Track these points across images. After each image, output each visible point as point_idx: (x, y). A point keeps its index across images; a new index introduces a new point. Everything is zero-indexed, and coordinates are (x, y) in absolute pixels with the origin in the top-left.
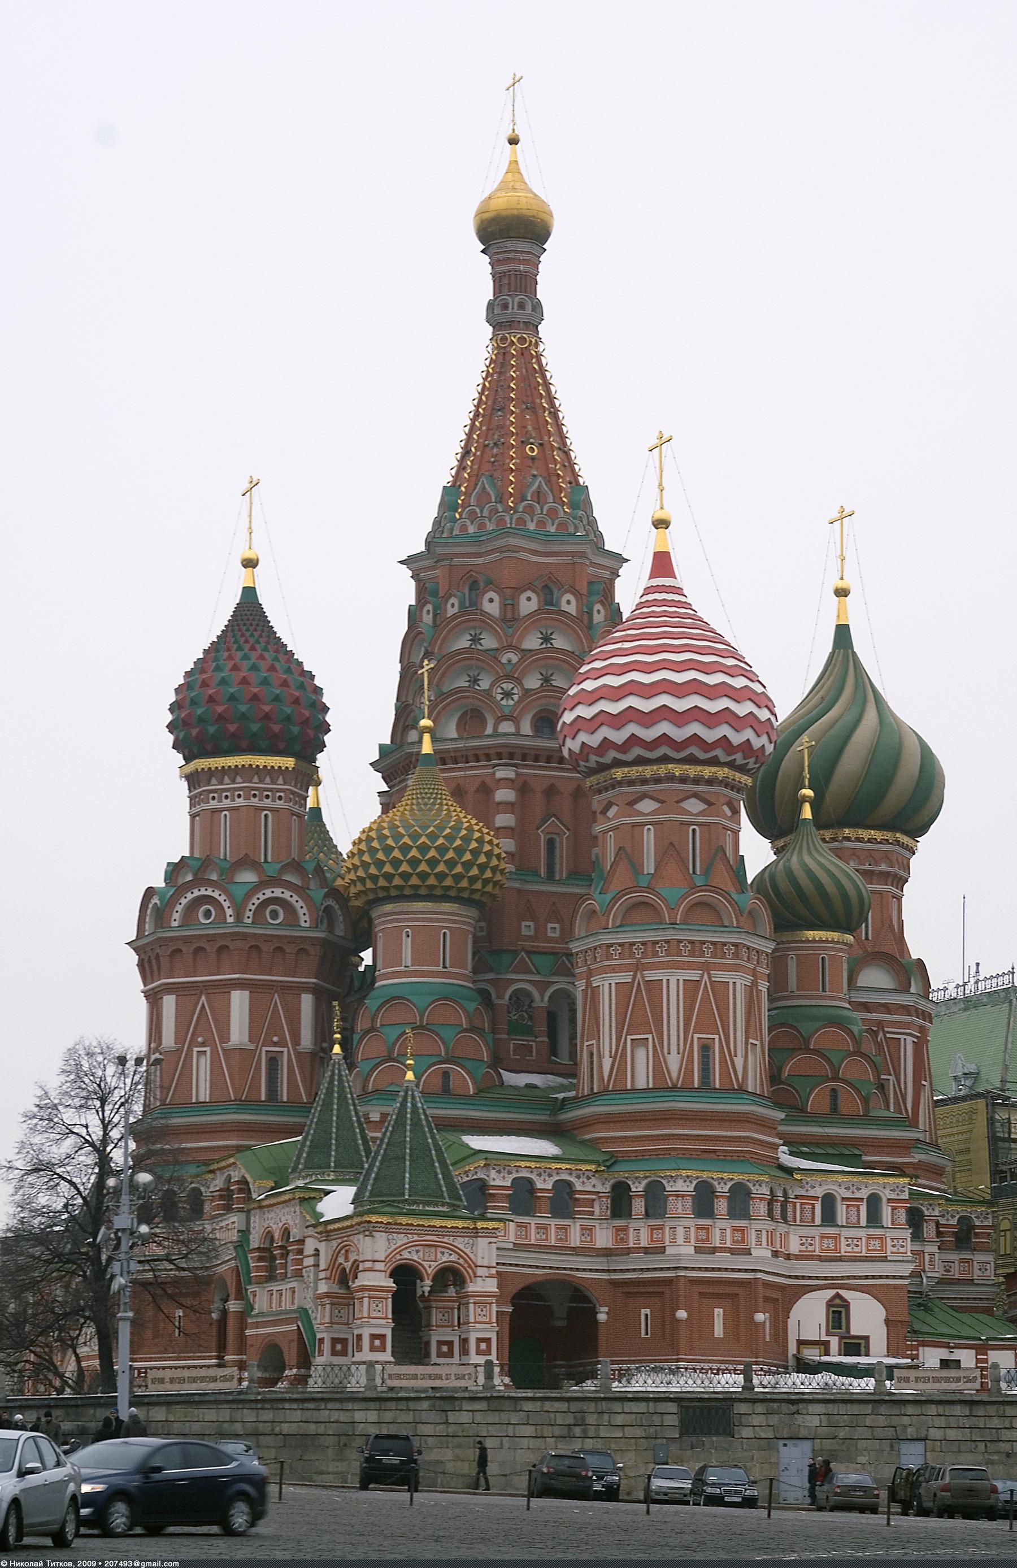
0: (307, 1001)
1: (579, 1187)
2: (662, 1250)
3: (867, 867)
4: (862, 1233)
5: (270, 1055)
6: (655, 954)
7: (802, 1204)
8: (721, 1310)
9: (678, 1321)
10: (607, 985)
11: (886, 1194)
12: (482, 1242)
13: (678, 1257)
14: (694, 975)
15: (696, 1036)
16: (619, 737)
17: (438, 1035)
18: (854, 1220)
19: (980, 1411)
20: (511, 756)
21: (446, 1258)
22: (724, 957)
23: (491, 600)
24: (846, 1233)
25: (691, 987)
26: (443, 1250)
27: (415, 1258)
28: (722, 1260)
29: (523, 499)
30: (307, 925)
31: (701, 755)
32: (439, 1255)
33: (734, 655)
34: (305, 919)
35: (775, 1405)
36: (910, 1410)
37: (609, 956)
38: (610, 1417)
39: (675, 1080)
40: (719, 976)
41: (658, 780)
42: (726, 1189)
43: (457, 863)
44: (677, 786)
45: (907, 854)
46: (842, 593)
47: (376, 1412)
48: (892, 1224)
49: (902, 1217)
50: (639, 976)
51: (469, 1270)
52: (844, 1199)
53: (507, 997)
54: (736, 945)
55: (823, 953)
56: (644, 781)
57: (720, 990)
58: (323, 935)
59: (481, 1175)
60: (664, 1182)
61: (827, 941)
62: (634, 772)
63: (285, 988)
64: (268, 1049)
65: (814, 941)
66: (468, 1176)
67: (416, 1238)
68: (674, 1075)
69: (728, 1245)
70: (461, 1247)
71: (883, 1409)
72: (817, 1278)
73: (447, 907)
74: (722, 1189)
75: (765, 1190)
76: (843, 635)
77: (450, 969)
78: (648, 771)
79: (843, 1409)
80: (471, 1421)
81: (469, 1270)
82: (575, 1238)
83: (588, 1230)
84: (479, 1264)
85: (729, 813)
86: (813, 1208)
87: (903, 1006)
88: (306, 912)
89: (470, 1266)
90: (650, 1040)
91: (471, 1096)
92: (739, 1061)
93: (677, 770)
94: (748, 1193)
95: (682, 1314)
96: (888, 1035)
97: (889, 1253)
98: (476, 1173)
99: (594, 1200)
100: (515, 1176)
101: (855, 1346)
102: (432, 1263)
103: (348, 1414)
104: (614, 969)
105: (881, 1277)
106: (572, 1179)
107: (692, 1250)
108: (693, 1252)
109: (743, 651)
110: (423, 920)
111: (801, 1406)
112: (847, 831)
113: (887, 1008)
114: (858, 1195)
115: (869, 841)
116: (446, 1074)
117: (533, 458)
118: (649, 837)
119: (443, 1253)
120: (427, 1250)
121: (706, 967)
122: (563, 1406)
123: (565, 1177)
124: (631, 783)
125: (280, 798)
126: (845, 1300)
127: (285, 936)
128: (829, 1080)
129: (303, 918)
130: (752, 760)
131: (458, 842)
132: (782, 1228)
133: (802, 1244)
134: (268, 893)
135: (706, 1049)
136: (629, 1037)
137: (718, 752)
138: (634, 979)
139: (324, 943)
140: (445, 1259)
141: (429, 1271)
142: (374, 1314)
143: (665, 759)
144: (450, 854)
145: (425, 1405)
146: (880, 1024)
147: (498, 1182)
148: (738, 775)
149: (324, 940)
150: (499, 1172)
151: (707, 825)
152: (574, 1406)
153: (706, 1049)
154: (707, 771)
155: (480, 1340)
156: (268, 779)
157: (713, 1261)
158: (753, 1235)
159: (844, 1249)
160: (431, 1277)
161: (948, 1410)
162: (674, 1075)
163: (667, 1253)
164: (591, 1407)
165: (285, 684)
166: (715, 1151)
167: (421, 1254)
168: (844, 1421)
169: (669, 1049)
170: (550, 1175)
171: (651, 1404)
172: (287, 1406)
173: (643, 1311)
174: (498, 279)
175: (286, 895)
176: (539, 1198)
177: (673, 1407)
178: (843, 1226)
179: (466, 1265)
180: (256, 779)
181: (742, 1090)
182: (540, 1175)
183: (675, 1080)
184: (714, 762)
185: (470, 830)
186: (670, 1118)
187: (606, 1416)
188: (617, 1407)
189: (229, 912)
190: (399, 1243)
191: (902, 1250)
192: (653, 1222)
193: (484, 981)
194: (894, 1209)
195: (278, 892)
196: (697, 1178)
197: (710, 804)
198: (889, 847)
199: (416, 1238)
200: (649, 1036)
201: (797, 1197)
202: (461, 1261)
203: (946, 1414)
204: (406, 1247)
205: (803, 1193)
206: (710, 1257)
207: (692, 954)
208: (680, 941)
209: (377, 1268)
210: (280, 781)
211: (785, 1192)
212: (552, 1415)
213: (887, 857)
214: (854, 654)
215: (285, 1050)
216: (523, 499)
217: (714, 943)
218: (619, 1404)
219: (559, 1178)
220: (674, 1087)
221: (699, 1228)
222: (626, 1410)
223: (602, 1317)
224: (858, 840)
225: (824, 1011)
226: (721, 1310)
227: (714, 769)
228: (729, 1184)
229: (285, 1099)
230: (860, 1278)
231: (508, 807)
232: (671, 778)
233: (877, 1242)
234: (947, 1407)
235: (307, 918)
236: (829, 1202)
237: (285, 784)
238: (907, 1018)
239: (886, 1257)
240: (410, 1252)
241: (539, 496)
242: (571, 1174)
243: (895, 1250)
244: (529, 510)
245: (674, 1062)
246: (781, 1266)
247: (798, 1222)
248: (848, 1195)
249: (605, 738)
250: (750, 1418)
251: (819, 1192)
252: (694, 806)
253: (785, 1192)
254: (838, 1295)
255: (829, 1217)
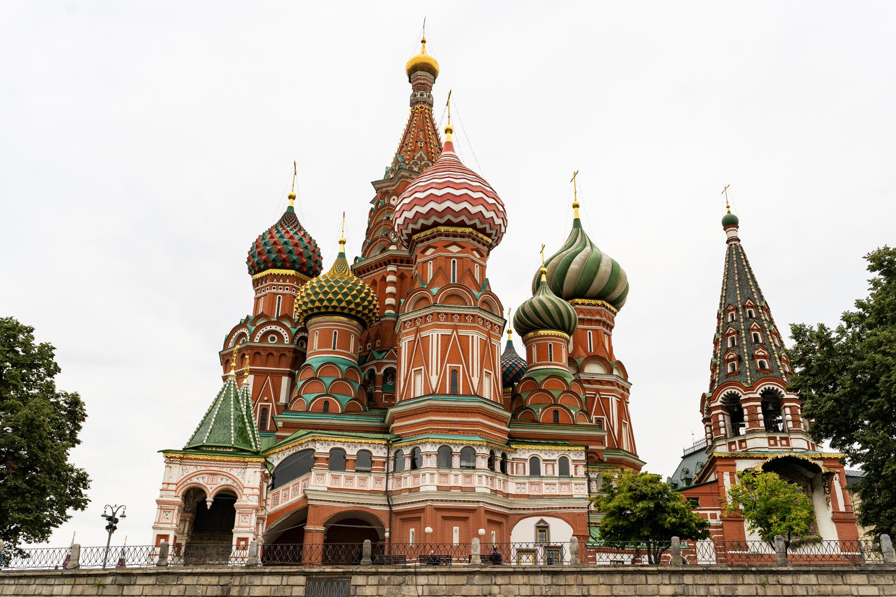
0: (285, 380)
1: (374, 454)
2: (417, 489)
3: (589, 317)
4: (556, 481)
5: (262, 407)
6: (426, 322)
7: (517, 464)
8: (458, 528)
9: (426, 534)
10: (404, 345)
11: (572, 457)
12: (250, 471)
13: (427, 493)
14: (448, 332)
15: (448, 365)
16: (410, 215)
17: (323, 381)
18: (550, 473)
19: (561, 580)
20: (395, 261)
21: (221, 482)
22: (466, 321)
23: (394, 200)
24: (545, 481)
25: (446, 339)
26: (222, 477)
27: (201, 482)
28: (456, 494)
29: (413, 159)
30: (288, 343)
31: (456, 221)
32: (219, 480)
33: (496, 198)
34: (287, 340)
35: (386, 578)
36: (500, 580)
37: (405, 328)
38: (250, 589)
39: (434, 390)
40: (462, 332)
41: (434, 237)
42: (459, 450)
43: (352, 302)
44: (443, 238)
45: (613, 315)
46: (576, 206)
47: (70, 587)
48: (576, 474)
49: (581, 471)
50: (418, 335)
51: (241, 491)
52: (544, 460)
53: (382, 372)
54: (473, 316)
55: (550, 342)
56: (428, 239)
57: (464, 340)
58: (293, 346)
59: (311, 446)
60: (420, 447)
61: (552, 336)
62: (422, 234)
63: (272, 373)
64: (261, 404)
65: (544, 336)
66: (302, 447)
67: (203, 468)
68: (434, 387)
69: (460, 485)
70: (236, 475)
71: (477, 579)
72: (528, 509)
73: (336, 318)
74: (457, 450)
75: (486, 451)
76: (577, 223)
77: (336, 350)
78: (429, 232)
79: (442, 580)
80: (140, 594)
81: (241, 491)
82: (371, 483)
83: (378, 480)
84: (246, 486)
85: (478, 256)
86: (524, 466)
87: (609, 382)
88: (288, 337)
89: (240, 488)
90: (423, 370)
91: (339, 414)
92: (475, 380)
93: (443, 229)
94: (475, 455)
95: (429, 530)
96: (602, 396)
97: (573, 492)
98: (308, 445)
99: (384, 463)
100: (332, 446)
101: (554, 552)
102: (213, 486)
103: (50, 588)
104: (407, 334)
105: (569, 508)
106: (370, 449)
107: (435, 489)
108: (436, 489)
109: (499, 194)
110: (324, 326)
111: (407, 578)
112: (577, 300)
113: (600, 382)
114: (552, 458)
115: (588, 305)
116: (327, 403)
117: (421, 147)
118: (430, 268)
119: (222, 479)
120: (211, 477)
121: (455, 328)
122: (214, 580)
123: (366, 447)
124: (422, 241)
125: (287, 289)
126: (545, 523)
127: (274, 347)
128: (552, 405)
129: (286, 340)
130: (487, 226)
131: (355, 292)
132: (501, 477)
133: (518, 488)
134: (268, 328)
135: (454, 372)
136: (413, 370)
137: (463, 218)
138: (415, 338)
139: (295, 351)
140: (223, 483)
141: (211, 491)
142: (164, 521)
143: (436, 224)
144: (349, 298)
145: (109, 580)
146: (598, 391)
147: (321, 450)
148: (480, 235)
149: (294, 349)
150: (322, 444)
151: (462, 258)
152: (224, 580)
153: (454, 372)
154: (459, 230)
155: (240, 539)
156: (281, 280)
157: (451, 496)
158: (476, 479)
159: (545, 491)
160: (213, 496)
161: (533, 579)
162: (434, 387)
163: (420, 491)
164: (237, 581)
165: (306, 247)
166: (457, 430)
167: (206, 480)
168: (443, 591)
169: (432, 373)
170: (355, 447)
171: (285, 578)
172: (7, 581)
173: (411, 530)
174: (416, 88)
175: (278, 329)
176: (348, 460)
177: (302, 580)
178: (543, 477)
179: (238, 487)
180: (275, 280)
181: (478, 396)
182: (349, 446)
183: (434, 390)
184: (462, 224)
185: (367, 294)
186: (430, 411)
187: (247, 589)
188: (257, 580)
189: (249, 338)
190: (190, 472)
191: (582, 491)
192: (414, 472)
193: (372, 365)
194: (576, 466)
195: (273, 328)
196: (440, 443)
197: (463, 247)
198: (599, 308)
199: (203, 468)
200: (422, 367)
201: (513, 459)
202: (235, 485)
203: (531, 583)
204: (196, 475)
205: (516, 456)
206: (448, 493)
207: (446, 320)
208: (439, 313)
209: (169, 489)
210: (288, 281)
211: (504, 455)
212: (205, 588)
213: (599, 313)
214: (583, 233)
215: (271, 404)
216: (413, 159)
217: (459, 315)
218: (259, 577)
219: (361, 448)
220: (434, 394)
221: (441, 475)
222: (265, 583)
223: (387, 535)
224: (583, 304)
225: (550, 371)
226: (458, 528)
227: (463, 229)
228: (461, 447)
229: (268, 429)
230: (556, 508)
231: (393, 283)
232: (441, 235)
233: (566, 487)
234: (532, 577)
235: (288, 339)
236: (535, 463)
237: (290, 282)
238: (612, 388)
239: (572, 495)
240: (198, 479)
241: (421, 159)
242: (370, 446)
243: (577, 491)
244: (416, 164)
245: (434, 380)
246: (499, 500)
247: (515, 474)
248: (546, 458)
249: (406, 217)
250: (364, 588)
251: (527, 456)
252: (454, 249)
253: (504, 455)
254: (542, 521)
255: (535, 470)
